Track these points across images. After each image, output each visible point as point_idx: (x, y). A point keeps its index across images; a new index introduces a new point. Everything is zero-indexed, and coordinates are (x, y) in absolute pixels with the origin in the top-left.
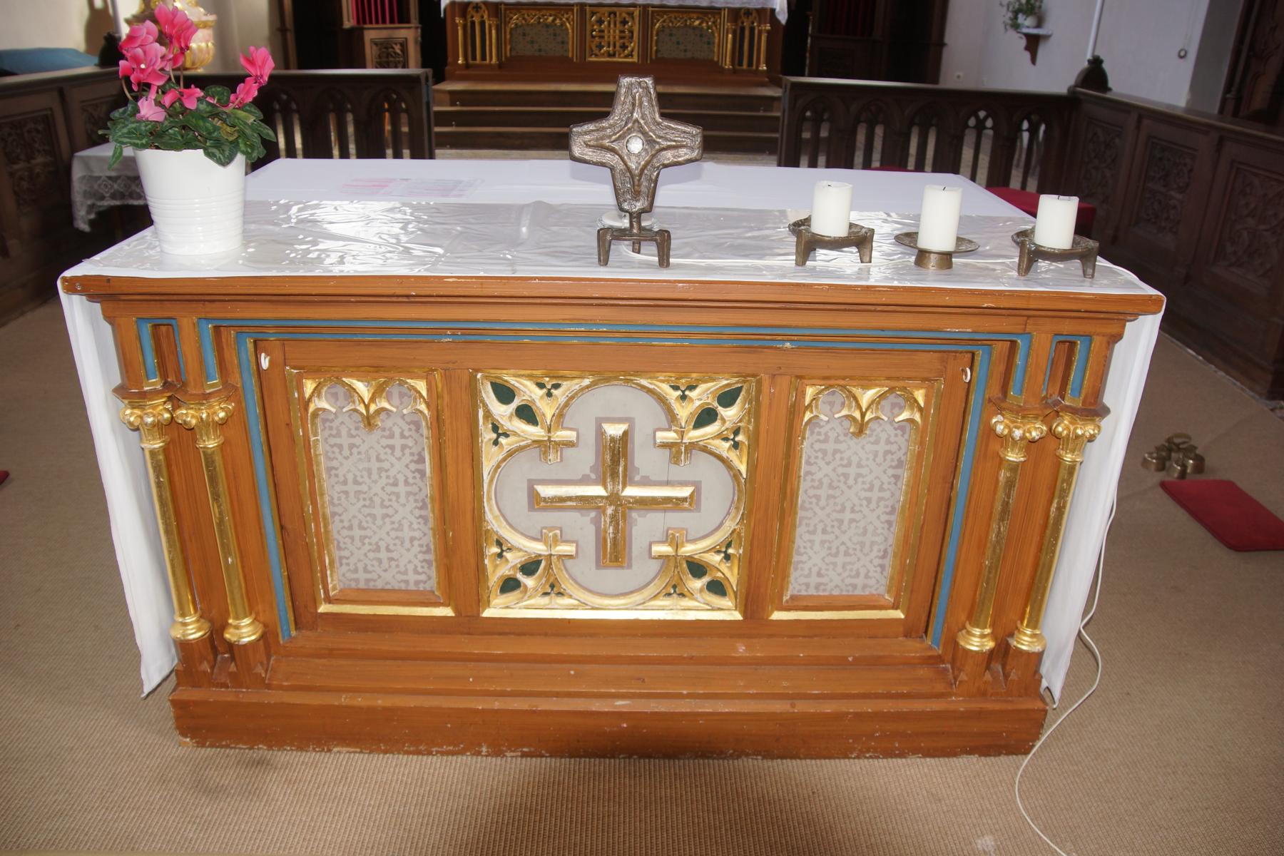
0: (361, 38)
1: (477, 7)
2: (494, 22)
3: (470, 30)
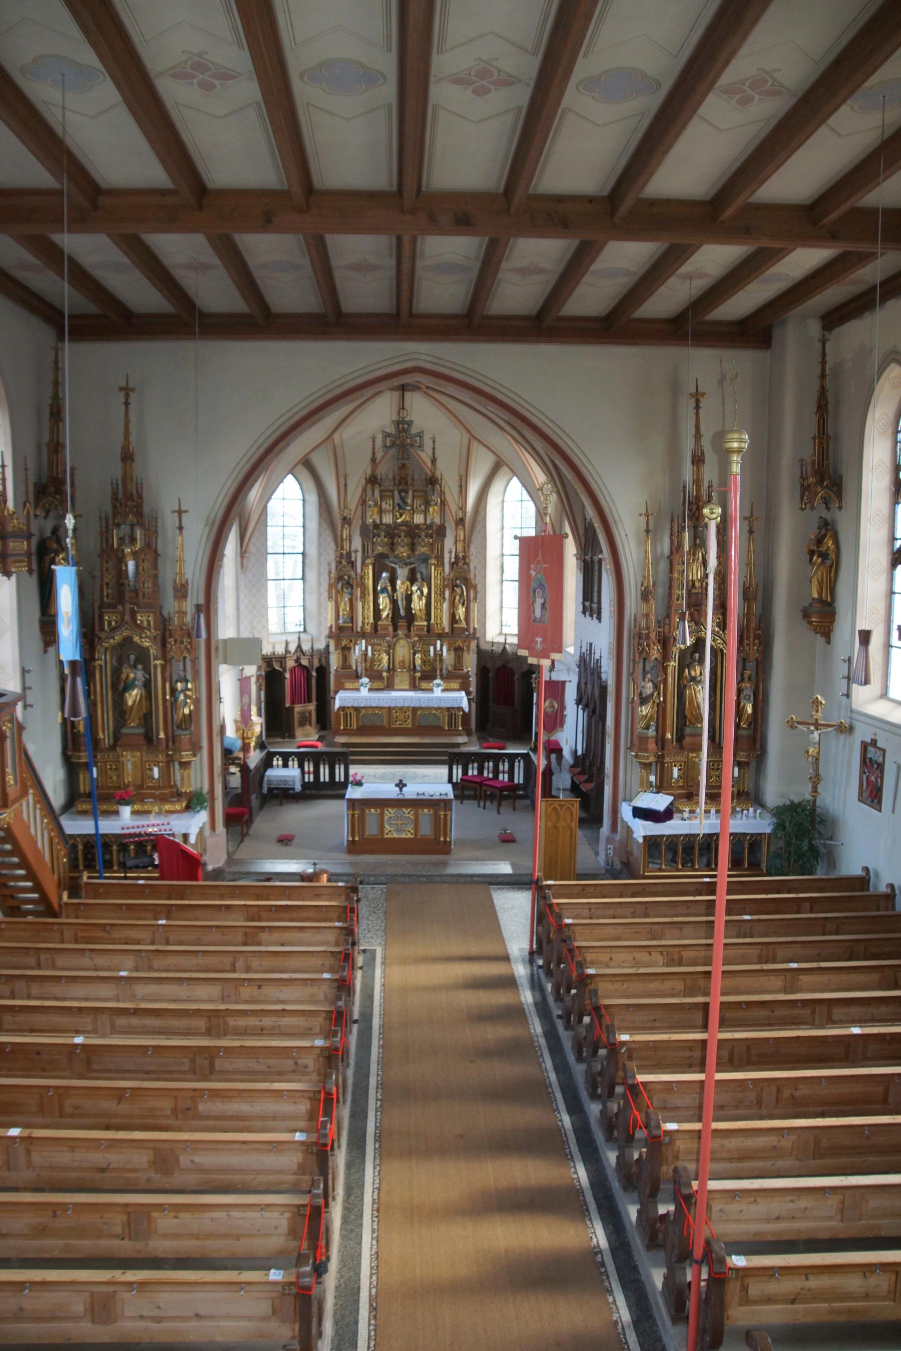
0: (293, 711)
1: (348, 708)
2: (355, 713)
3: (346, 716)
